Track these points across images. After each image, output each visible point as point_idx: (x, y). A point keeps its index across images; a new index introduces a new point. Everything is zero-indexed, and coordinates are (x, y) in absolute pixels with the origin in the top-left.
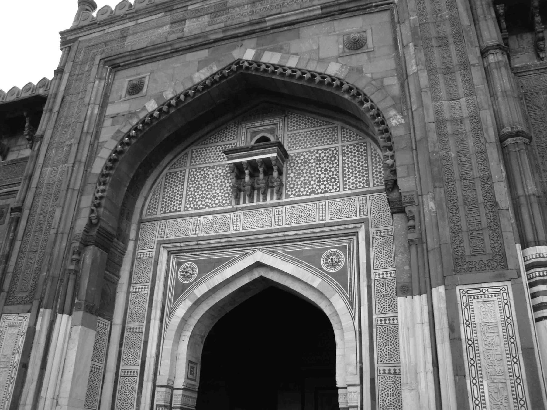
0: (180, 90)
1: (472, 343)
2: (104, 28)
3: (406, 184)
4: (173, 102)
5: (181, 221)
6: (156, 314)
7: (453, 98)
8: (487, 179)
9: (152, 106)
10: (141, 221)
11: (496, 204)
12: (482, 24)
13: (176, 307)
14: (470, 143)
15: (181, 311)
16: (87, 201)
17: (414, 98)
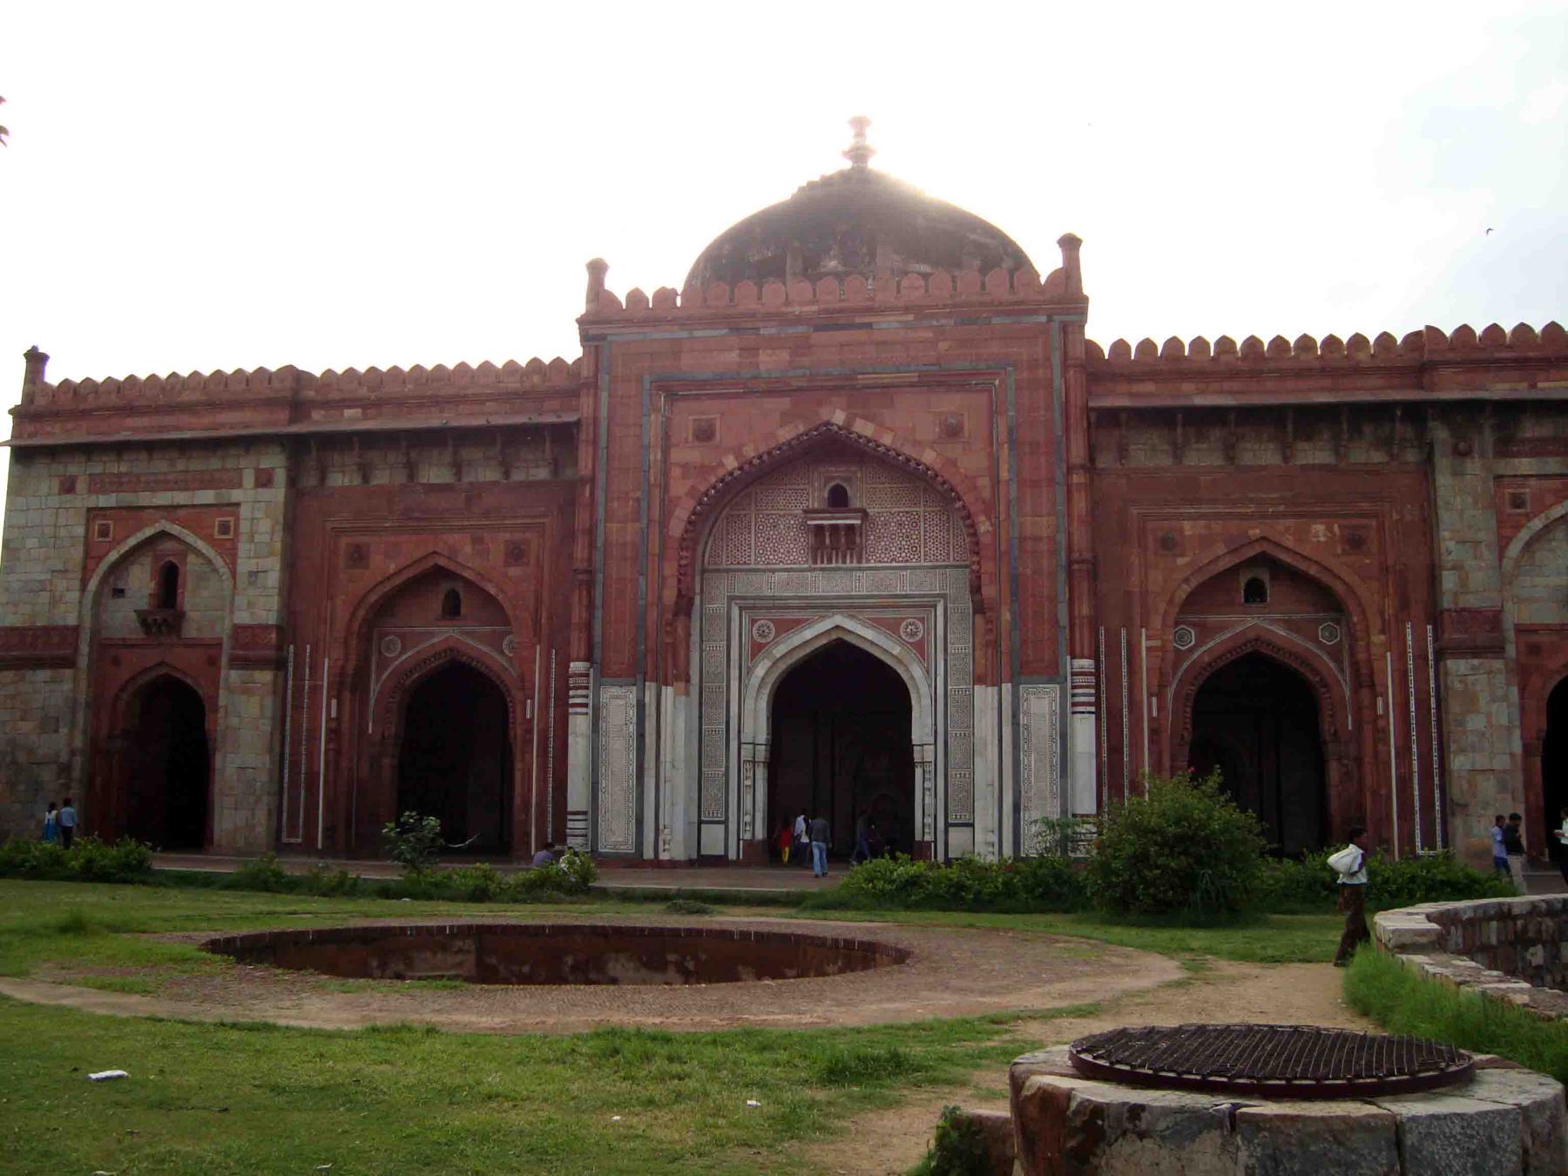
0: (763, 449)
1: (1027, 727)
2: (646, 330)
3: (988, 591)
4: (756, 461)
5: (753, 577)
6: (735, 673)
7: (1036, 514)
8: (1053, 600)
9: (731, 463)
10: (704, 571)
11: (1057, 622)
12: (1073, 436)
13: (755, 666)
14: (1045, 562)
15: (760, 671)
16: (670, 569)
17: (1002, 508)
